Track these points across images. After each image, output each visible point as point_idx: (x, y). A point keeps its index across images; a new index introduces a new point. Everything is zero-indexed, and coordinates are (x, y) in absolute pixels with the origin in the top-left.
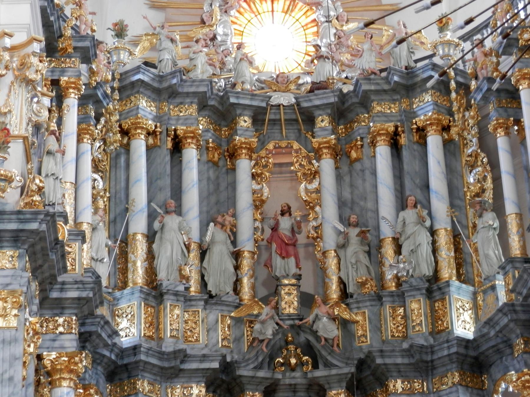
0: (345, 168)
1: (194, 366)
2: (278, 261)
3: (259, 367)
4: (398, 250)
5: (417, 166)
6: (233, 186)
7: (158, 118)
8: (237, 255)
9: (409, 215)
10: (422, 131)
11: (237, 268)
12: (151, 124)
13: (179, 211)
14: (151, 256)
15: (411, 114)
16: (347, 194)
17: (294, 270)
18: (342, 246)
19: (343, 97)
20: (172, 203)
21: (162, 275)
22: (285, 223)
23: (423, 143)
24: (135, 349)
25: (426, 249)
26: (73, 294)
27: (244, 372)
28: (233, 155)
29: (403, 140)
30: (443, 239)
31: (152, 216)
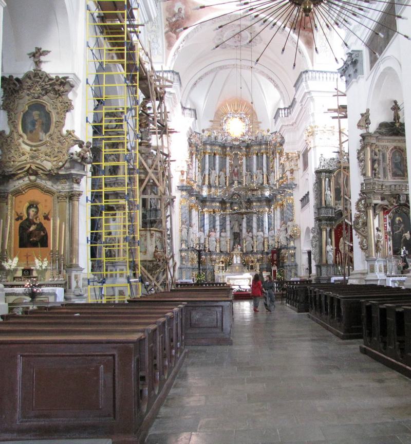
0: (248, 158)
1: (217, 200)
2: (234, 177)
3: (229, 199)
4: (256, 177)
5: (261, 160)
6: (226, 162)
7: (211, 150)
8: (226, 177)
9: (259, 171)
10: (262, 153)
11: (226, 179)
12: (209, 151)
13: (215, 169)
14: (209, 178)
15: (260, 150)
16: (248, 164)
17: (237, 179)
18: (246, 175)
19: (248, 144)
20: (213, 168)
21: (211, 183)
22: (236, 169)
23: (262, 156)
24: (206, 198)
25: (261, 178)
26: (195, 193)
27: (227, 201)
28: (226, 155)
29: (259, 154)
30: (265, 176)
31: (209, 170)
